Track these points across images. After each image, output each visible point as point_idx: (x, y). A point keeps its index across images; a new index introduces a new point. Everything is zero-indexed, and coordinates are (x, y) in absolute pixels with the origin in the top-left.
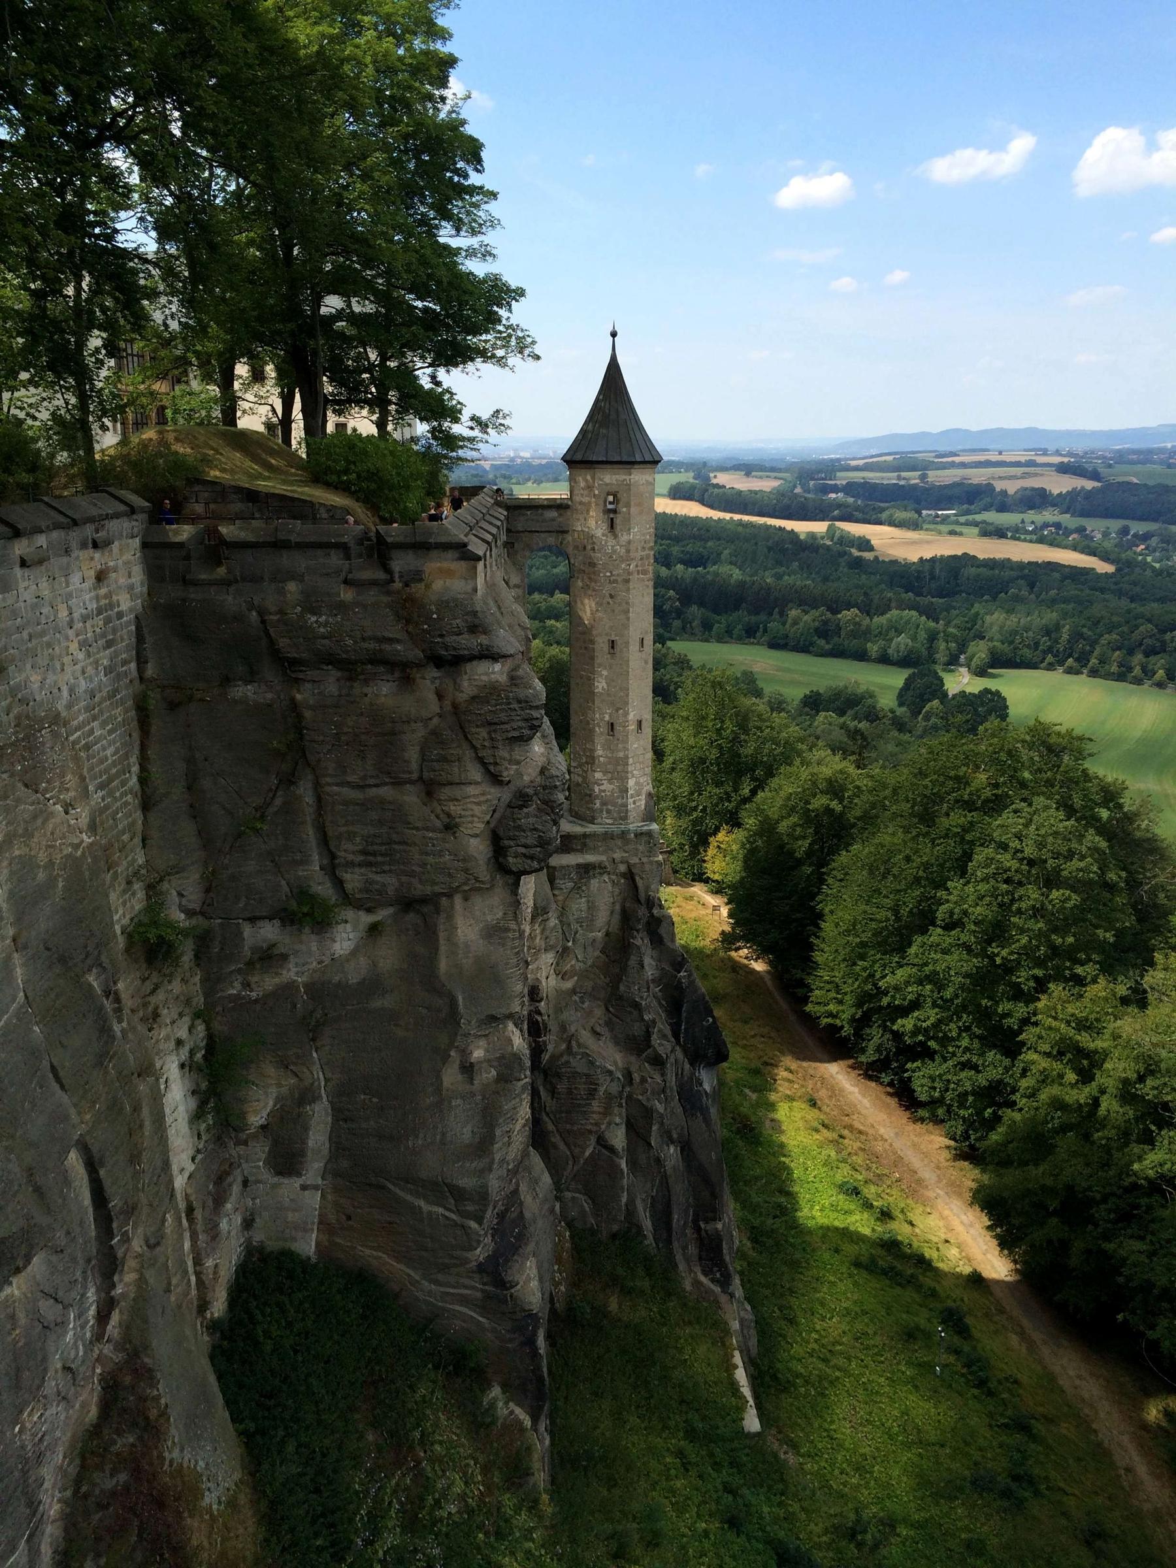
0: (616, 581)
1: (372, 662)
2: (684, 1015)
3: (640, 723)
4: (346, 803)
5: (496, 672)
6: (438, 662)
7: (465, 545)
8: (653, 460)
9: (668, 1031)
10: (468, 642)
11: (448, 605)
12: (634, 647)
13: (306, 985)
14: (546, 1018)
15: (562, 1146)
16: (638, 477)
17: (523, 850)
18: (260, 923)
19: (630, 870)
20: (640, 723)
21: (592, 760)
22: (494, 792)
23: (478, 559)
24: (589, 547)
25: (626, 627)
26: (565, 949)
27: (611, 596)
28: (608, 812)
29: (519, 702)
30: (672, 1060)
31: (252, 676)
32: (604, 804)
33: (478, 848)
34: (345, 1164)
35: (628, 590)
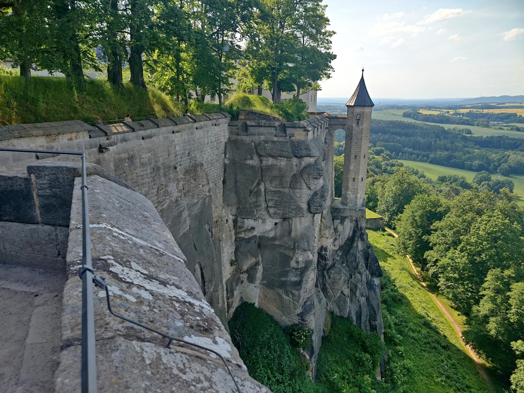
0: (358, 139)
1: (280, 156)
2: (369, 262)
3: (362, 179)
4: (272, 191)
5: (312, 160)
6: (296, 157)
7: (305, 128)
8: (372, 105)
9: (364, 265)
10: (304, 152)
11: (300, 142)
12: (362, 157)
13: (259, 236)
14: (328, 256)
15: (331, 292)
16: (367, 110)
17: (315, 207)
18: (249, 220)
19: (356, 219)
20: (362, 179)
21: (347, 188)
22: (309, 192)
23: (309, 131)
24: (351, 129)
25: (360, 152)
26: (336, 239)
27: (356, 143)
28: (352, 203)
29: (317, 169)
30: (365, 273)
31: (252, 158)
32: (350, 200)
33: (304, 206)
34: (265, 282)
35: (361, 141)
